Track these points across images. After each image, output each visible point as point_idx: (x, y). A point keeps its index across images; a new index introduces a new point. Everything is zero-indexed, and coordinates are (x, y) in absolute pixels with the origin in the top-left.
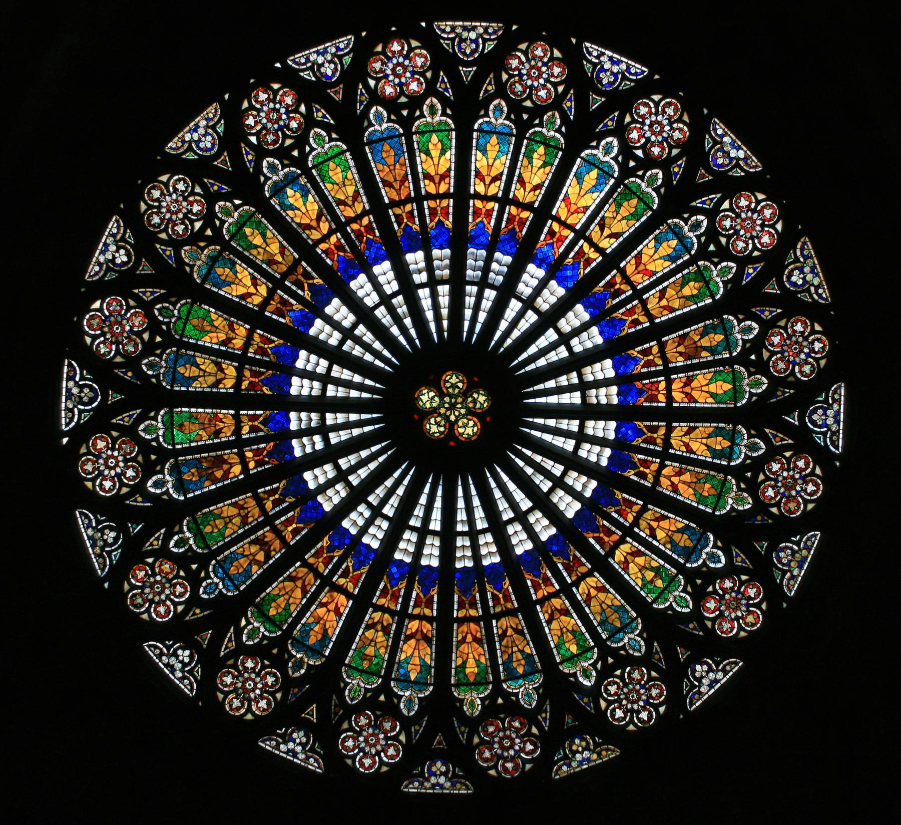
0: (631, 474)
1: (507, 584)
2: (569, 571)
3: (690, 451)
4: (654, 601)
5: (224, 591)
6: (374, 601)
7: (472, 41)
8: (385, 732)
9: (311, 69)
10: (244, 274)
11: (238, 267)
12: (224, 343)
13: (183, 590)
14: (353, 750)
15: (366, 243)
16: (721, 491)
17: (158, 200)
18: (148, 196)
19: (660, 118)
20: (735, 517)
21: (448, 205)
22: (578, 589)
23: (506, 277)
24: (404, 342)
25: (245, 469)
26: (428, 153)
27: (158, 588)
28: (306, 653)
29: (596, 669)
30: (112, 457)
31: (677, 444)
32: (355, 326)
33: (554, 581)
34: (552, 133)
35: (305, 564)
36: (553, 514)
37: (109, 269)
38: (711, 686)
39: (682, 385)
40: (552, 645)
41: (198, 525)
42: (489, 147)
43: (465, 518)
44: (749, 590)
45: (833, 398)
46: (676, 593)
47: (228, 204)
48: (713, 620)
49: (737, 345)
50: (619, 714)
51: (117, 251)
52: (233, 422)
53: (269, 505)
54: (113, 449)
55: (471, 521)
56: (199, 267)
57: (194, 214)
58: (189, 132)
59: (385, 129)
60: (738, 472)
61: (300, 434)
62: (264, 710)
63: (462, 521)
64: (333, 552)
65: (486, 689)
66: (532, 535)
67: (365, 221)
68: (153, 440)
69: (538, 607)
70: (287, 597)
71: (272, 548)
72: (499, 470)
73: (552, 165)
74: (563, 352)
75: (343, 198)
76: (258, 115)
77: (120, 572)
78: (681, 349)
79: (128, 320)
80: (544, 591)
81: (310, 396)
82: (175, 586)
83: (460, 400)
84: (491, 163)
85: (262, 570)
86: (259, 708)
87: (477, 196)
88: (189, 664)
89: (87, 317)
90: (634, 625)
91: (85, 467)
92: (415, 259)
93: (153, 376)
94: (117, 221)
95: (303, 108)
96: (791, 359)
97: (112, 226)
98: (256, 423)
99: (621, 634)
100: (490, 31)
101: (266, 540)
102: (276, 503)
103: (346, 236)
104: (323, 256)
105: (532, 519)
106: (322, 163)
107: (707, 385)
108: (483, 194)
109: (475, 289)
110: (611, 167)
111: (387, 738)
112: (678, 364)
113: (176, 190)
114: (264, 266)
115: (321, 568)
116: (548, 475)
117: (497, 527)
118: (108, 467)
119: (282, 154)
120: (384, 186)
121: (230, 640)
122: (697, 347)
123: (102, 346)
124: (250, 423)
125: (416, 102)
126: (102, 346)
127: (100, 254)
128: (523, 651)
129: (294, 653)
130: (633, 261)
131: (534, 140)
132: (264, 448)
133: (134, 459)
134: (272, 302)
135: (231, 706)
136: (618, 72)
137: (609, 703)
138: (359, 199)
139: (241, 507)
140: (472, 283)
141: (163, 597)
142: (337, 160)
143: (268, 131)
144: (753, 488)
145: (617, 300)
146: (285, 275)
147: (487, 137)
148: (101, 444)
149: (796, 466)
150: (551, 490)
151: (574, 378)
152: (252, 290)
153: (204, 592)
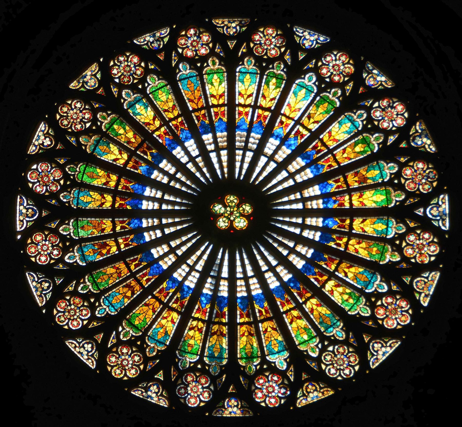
0: (332, 244)
1: (266, 305)
2: (301, 295)
3: (364, 231)
4: (349, 310)
5: (110, 313)
6: (193, 315)
7: (234, 28)
8: (202, 384)
9: (147, 44)
10: (114, 148)
11: (111, 145)
12: (105, 184)
13: (86, 313)
14: (184, 394)
15: (180, 131)
16: (383, 252)
17: (66, 112)
18: (61, 111)
19: (338, 62)
20: (391, 264)
21: (225, 110)
22: (306, 305)
23: (258, 145)
24: (204, 181)
25: (119, 248)
26: (212, 84)
27: (72, 313)
28: (156, 344)
29: (318, 347)
30: (45, 245)
31: (357, 228)
32: (176, 173)
33: (292, 302)
34: (279, 72)
35: (154, 297)
36: (290, 267)
37: (40, 148)
38: (384, 354)
39: (358, 197)
40: (293, 335)
41: (94, 279)
42: (245, 80)
43: (241, 270)
44: (402, 303)
45: (442, 201)
46: (361, 306)
47: (104, 114)
48: (383, 320)
49: (387, 176)
50: (333, 371)
51: (45, 139)
52: (111, 224)
53: (132, 267)
54: (46, 240)
55: (244, 272)
56: (90, 146)
57: (86, 119)
58: (82, 78)
59: (188, 73)
60: (391, 242)
61: (148, 229)
62: (134, 375)
63: (240, 272)
64: (169, 290)
65: (258, 360)
66: (279, 278)
67: (180, 120)
68: (67, 235)
69: (284, 315)
70: (144, 314)
71: (135, 289)
72: (259, 245)
73: (280, 87)
74: (291, 182)
75: (167, 108)
76: (119, 68)
77: (51, 305)
78: (356, 179)
79: (52, 174)
80: (287, 307)
81: (153, 210)
82: (82, 310)
83: (236, 209)
84: (246, 88)
85: (130, 301)
86: (131, 374)
87: (240, 105)
88: (91, 351)
89: (30, 173)
90: (338, 323)
91: (31, 250)
92: (207, 138)
93: (66, 202)
94: (45, 124)
95: (143, 64)
96: (417, 182)
97: (42, 126)
98: (124, 225)
99: (331, 329)
100: (243, 22)
101: (132, 285)
102: (136, 266)
103: (169, 127)
104: (157, 138)
105: (279, 269)
106: (155, 91)
107: (372, 197)
108: (243, 104)
109: (241, 152)
110: (312, 87)
111: (203, 388)
112: (355, 187)
113: (76, 107)
114: (125, 144)
115: (163, 299)
116: (286, 247)
117: (259, 275)
118: (42, 250)
119: (133, 88)
120: (189, 101)
121: (113, 338)
122: (365, 178)
123: (38, 187)
124: (121, 225)
125: (204, 59)
126: (38, 187)
127: (35, 141)
128: (277, 339)
129: (149, 344)
130: (327, 135)
131: (269, 76)
132: (129, 237)
133: (57, 245)
134: (130, 162)
135: (115, 373)
136: (314, 40)
137: (327, 365)
138: (176, 109)
139: (118, 269)
140: (239, 149)
141: (75, 317)
142: (163, 89)
143: (125, 76)
144: (399, 249)
145: (319, 155)
146: (137, 149)
147: (244, 75)
148: (39, 238)
149: (423, 238)
150: (288, 254)
151: (298, 196)
152: (119, 157)
153: (98, 313)
